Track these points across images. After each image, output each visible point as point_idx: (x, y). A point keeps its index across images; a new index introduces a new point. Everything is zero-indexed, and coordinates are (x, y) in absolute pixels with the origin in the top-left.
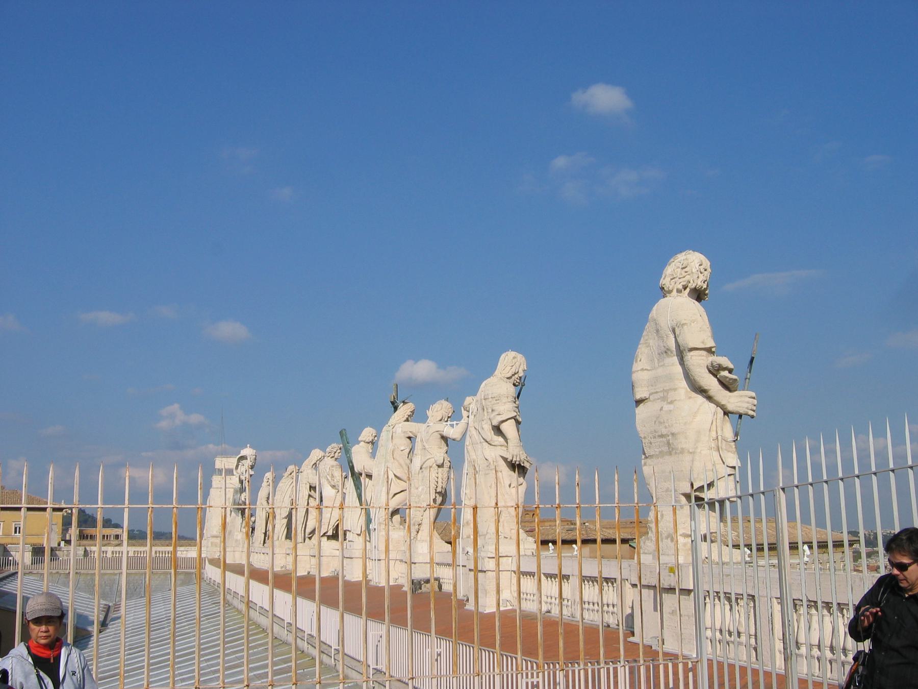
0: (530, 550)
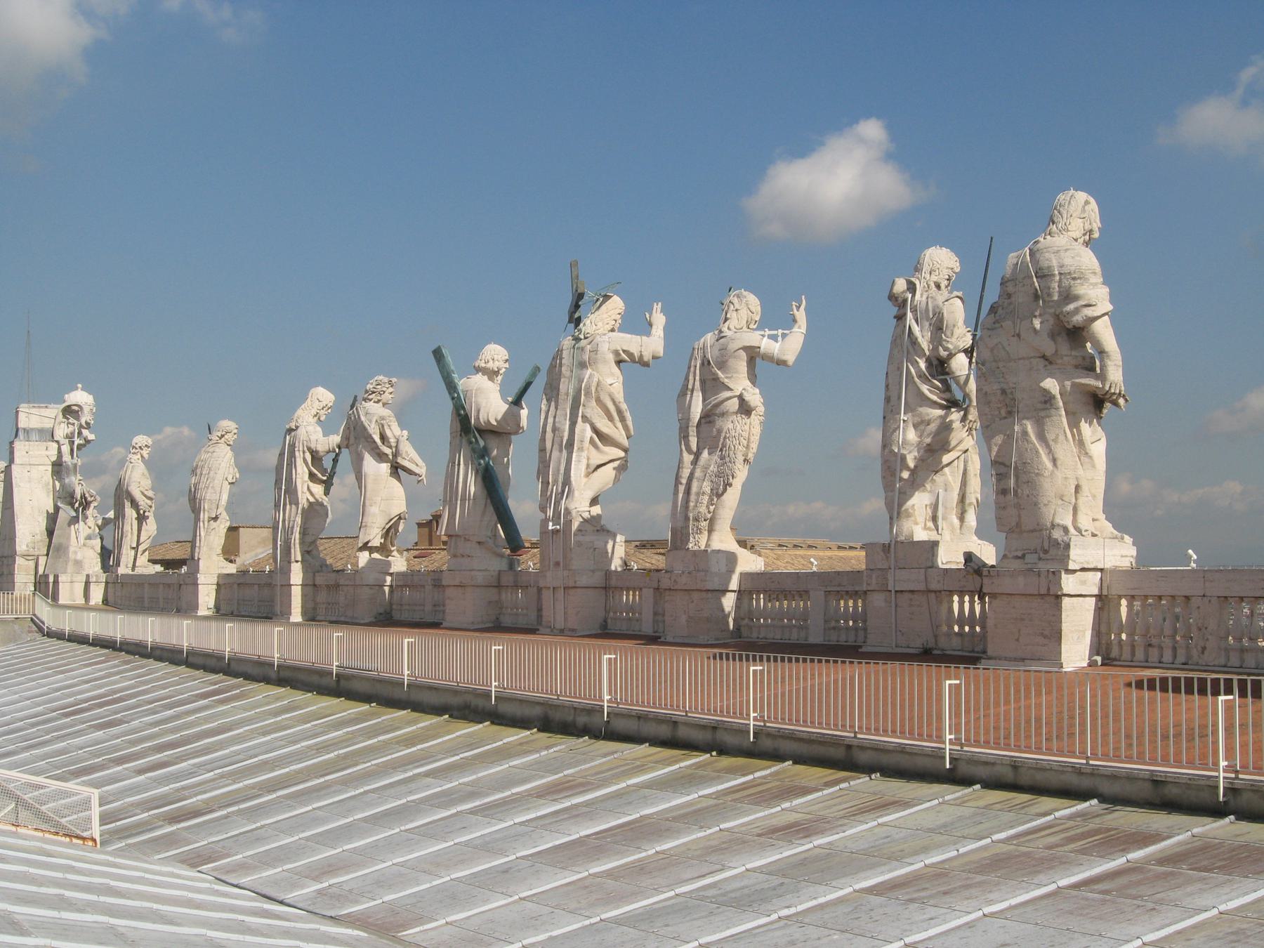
0: (1128, 559)
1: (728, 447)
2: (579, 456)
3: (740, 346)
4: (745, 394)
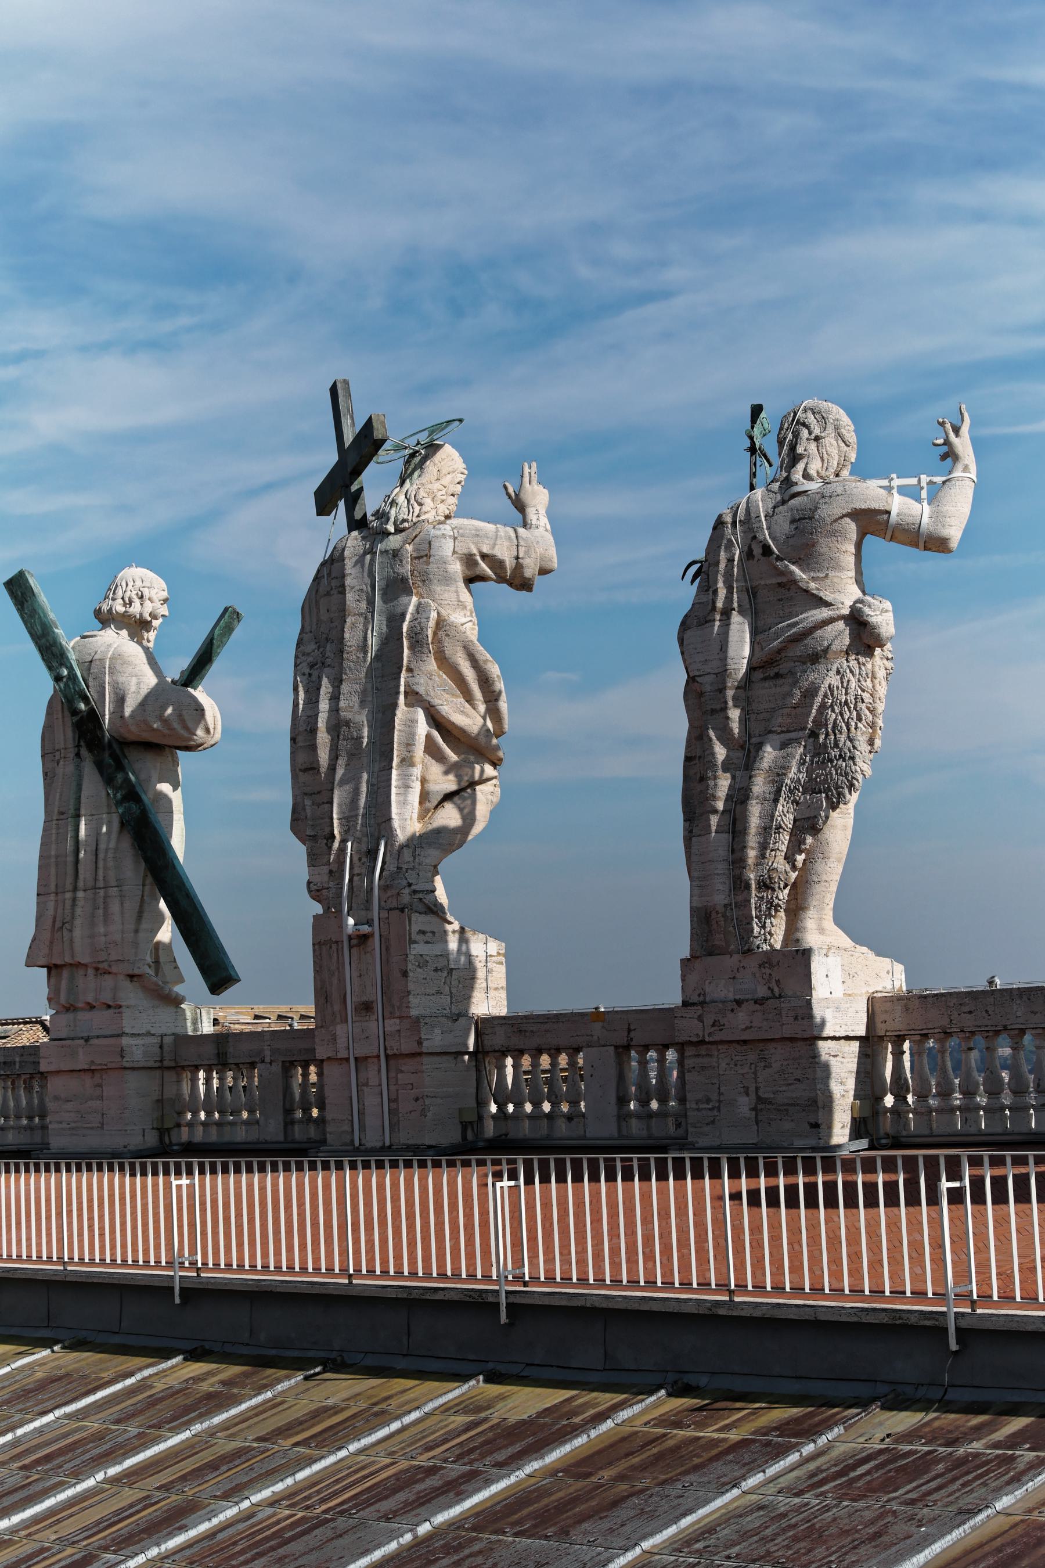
1: (830, 726)
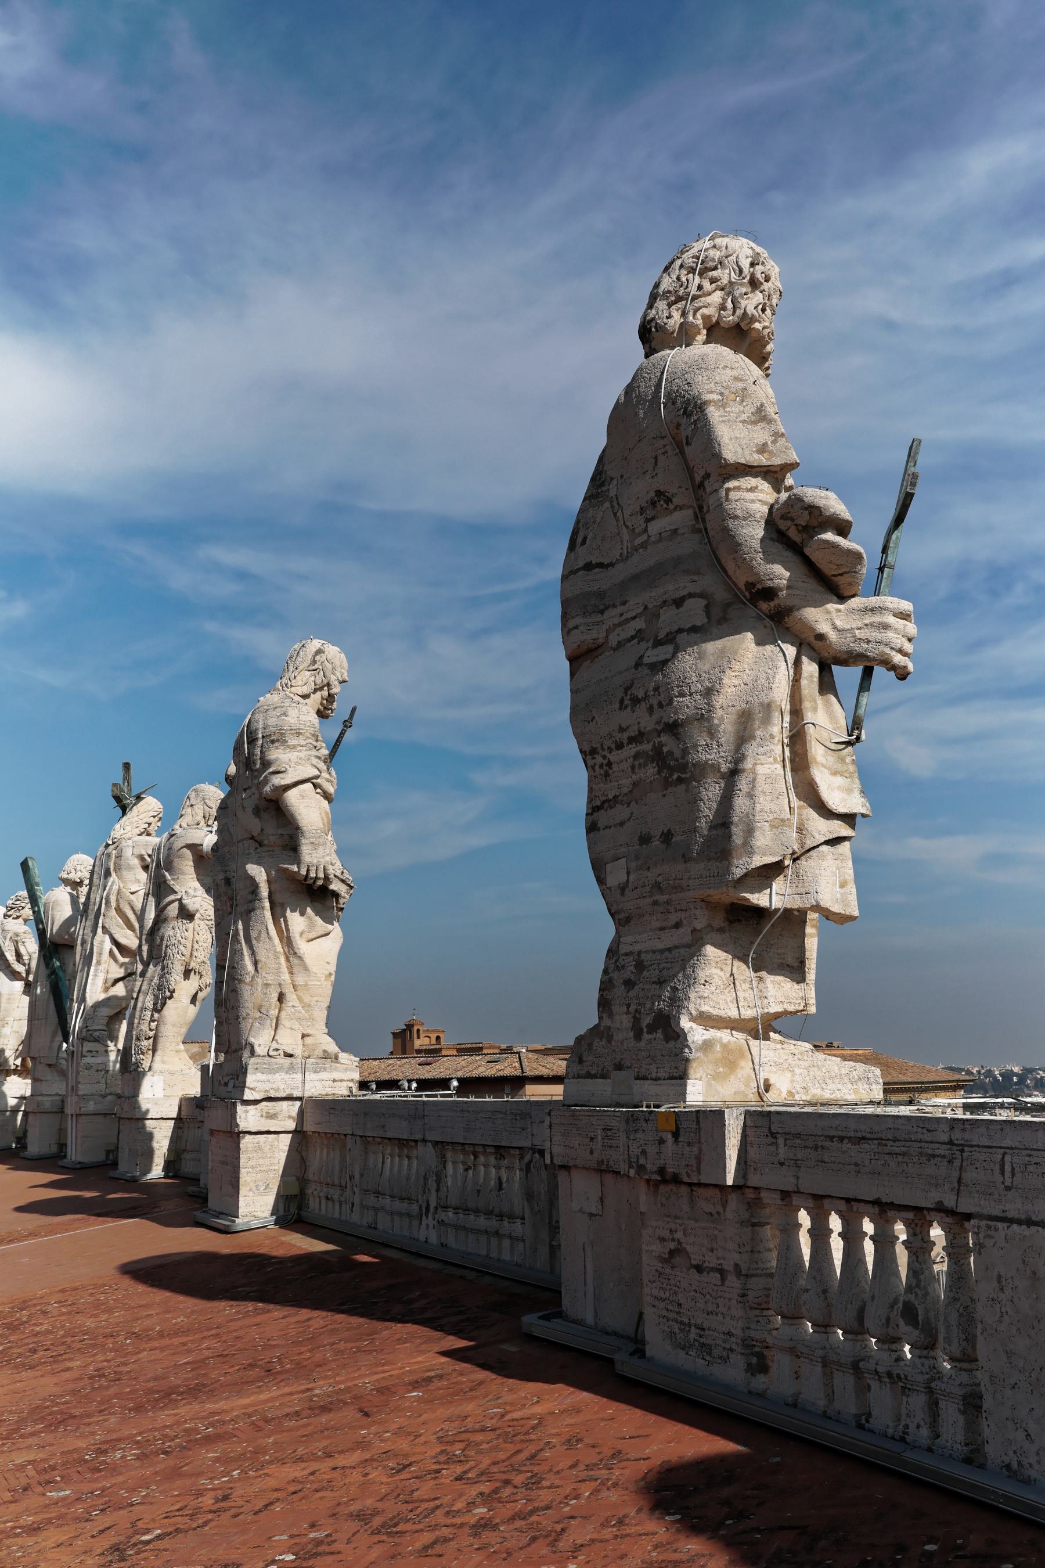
0: (344, 1084)
2: (96, 970)
3: (183, 845)
4: (184, 897)
